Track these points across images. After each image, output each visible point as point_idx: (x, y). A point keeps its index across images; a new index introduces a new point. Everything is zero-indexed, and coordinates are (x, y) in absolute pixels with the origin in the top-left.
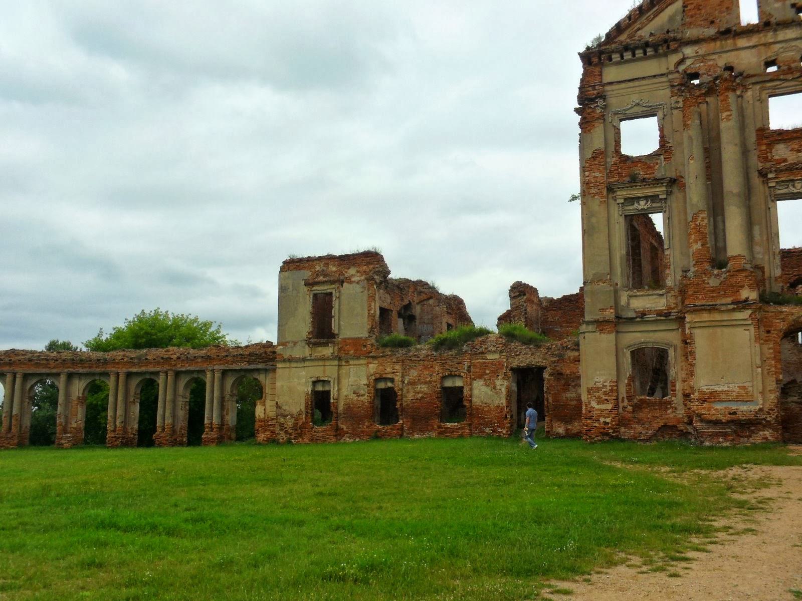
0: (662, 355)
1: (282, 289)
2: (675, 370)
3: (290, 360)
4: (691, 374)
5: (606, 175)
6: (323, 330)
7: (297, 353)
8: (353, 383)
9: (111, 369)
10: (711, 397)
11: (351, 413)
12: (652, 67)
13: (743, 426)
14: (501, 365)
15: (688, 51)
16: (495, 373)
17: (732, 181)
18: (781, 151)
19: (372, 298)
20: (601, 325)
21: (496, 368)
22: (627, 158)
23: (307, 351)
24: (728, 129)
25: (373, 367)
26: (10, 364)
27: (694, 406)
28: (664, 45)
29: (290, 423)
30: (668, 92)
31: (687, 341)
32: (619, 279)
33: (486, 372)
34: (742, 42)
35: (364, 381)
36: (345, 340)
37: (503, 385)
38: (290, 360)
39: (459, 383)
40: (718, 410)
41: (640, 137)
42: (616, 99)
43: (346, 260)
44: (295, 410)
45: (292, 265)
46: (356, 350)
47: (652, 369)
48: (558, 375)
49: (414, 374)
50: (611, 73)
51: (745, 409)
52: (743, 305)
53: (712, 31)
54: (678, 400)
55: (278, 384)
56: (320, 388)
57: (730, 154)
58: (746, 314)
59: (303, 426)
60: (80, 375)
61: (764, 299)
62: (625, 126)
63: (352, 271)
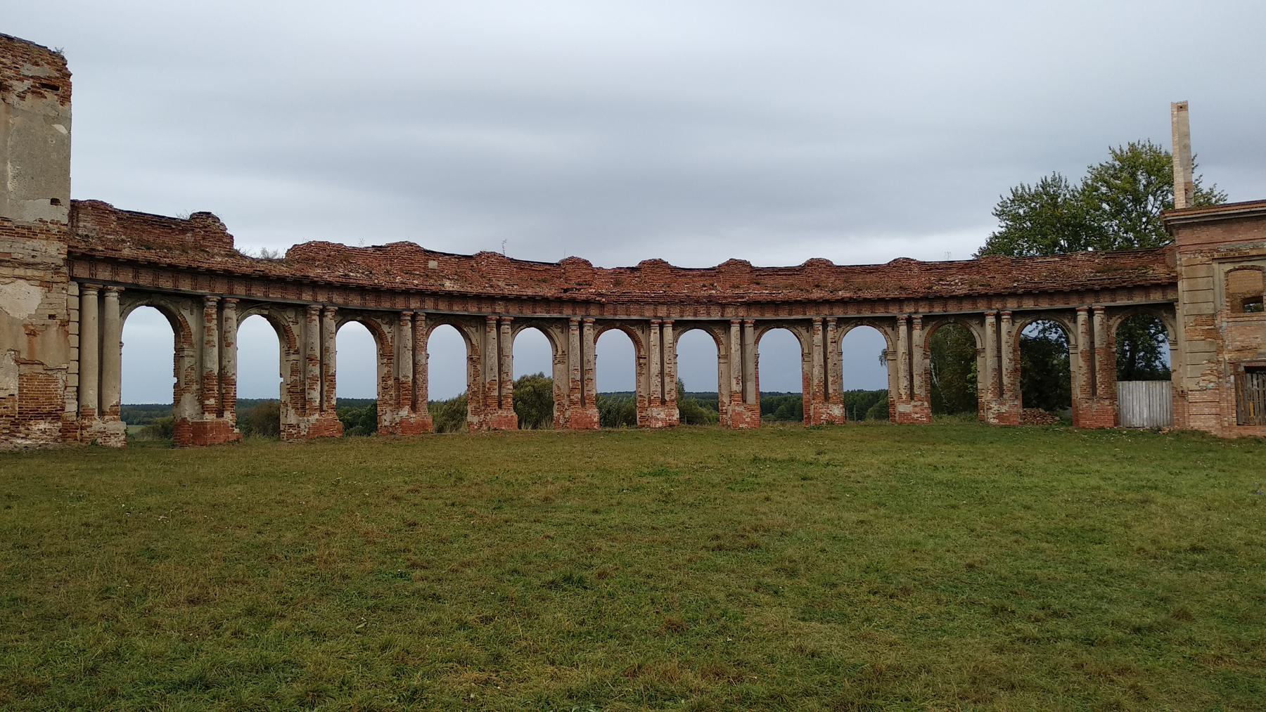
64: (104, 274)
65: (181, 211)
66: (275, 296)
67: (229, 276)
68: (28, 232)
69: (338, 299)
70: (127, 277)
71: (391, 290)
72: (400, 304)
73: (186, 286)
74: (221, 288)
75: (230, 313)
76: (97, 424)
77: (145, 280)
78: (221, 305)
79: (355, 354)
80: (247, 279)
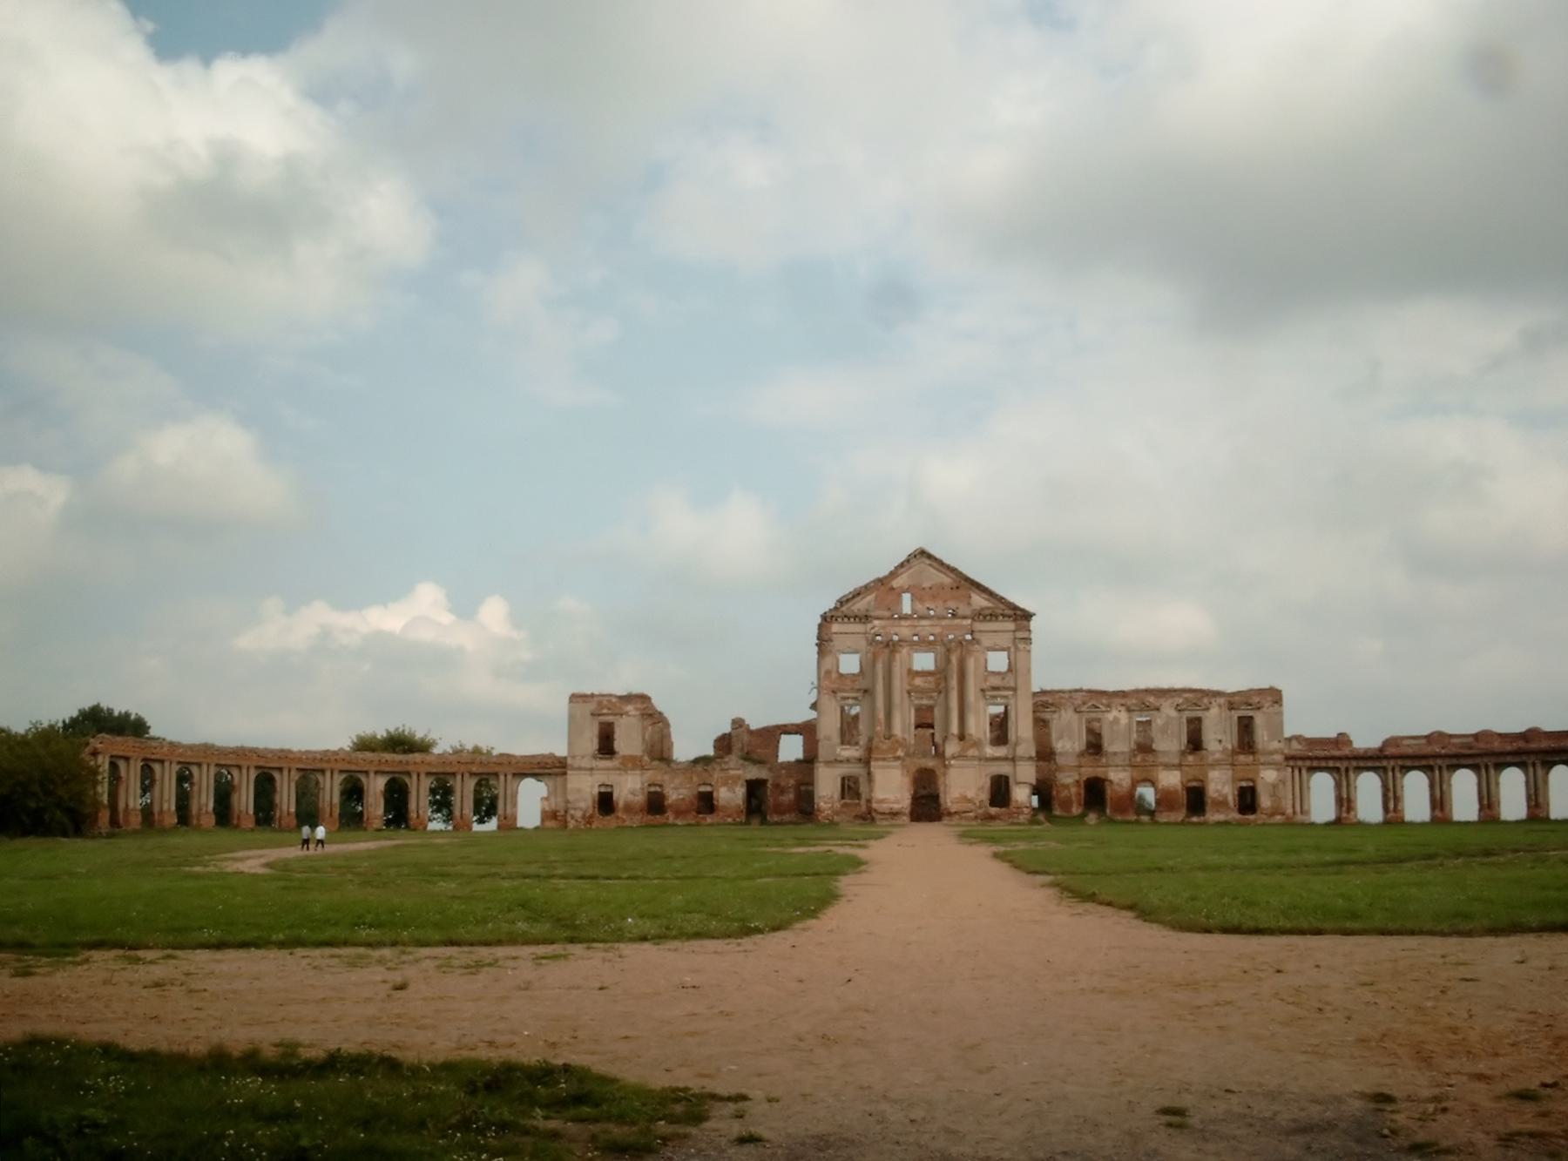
0: (855, 780)
1: (571, 717)
2: (863, 789)
3: (580, 769)
4: (871, 790)
5: (830, 683)
6: (606, 746)
7: (585, 763)
8: (629, 787)
9: (409, 768)
10: (882, 801)
11: (628, 808)
12: (859, 628)
13: (894, 814)
14: (739, 777)
15: (876, 622)
16: (735, 783)
17: (897, 698)
18: (918, 681)
19: (644, 729)
20: (828, 763)
21: (736, 779)
22: (841, 675)
23: (595, 763)
24: (898, 671)
25: (649, 775)
26: (328, 761)
27: (874, 805)
28: (865, 618)
29: (579, 814)
30: (864, 643)
31: (869, 774)
32: (836, 739)
33: (729, 782)
34: (903, 623)
35: (638, 786)
36: (624, 757)
37: (741, 791)
38: (580, 769)
39: (708, 789)
40: (884, 807)
41: (850, 664)
42: (838, 642)
43: (629, 698)
44: (582, 805)
45: (574, 698)
46: (632, 763)
47: (849, 788)
48: (776, 786)
49: (677, 781)
50: (835, 627)
51: (896, 807)
52: (898, 758)
53: (887, 614)
54: (863, 802)
55: (569, 786)
56: (603, 790)
57: (897, 683)
58: (898, 763)
59: (591, 817)
60: (383, 773)
61: (907, 755)
62: (843, 658)
63: (630, 708)
64: (1300, 763)
65: (1333, 735)
66: (1370, 764)
67: (1347, 758)
68: (1272, 753)
69: (1400, 762)
70: (1308, 763)
71: (1439, 756)
72: (1431, 763)
73: (1331, 764)
74: (1345, 764)
75: (1352, 775)
76: (1299, 818)
77: (1315, 764)
78: (1347, 770)
79: (1415, 787)
80: (1356, 758)
